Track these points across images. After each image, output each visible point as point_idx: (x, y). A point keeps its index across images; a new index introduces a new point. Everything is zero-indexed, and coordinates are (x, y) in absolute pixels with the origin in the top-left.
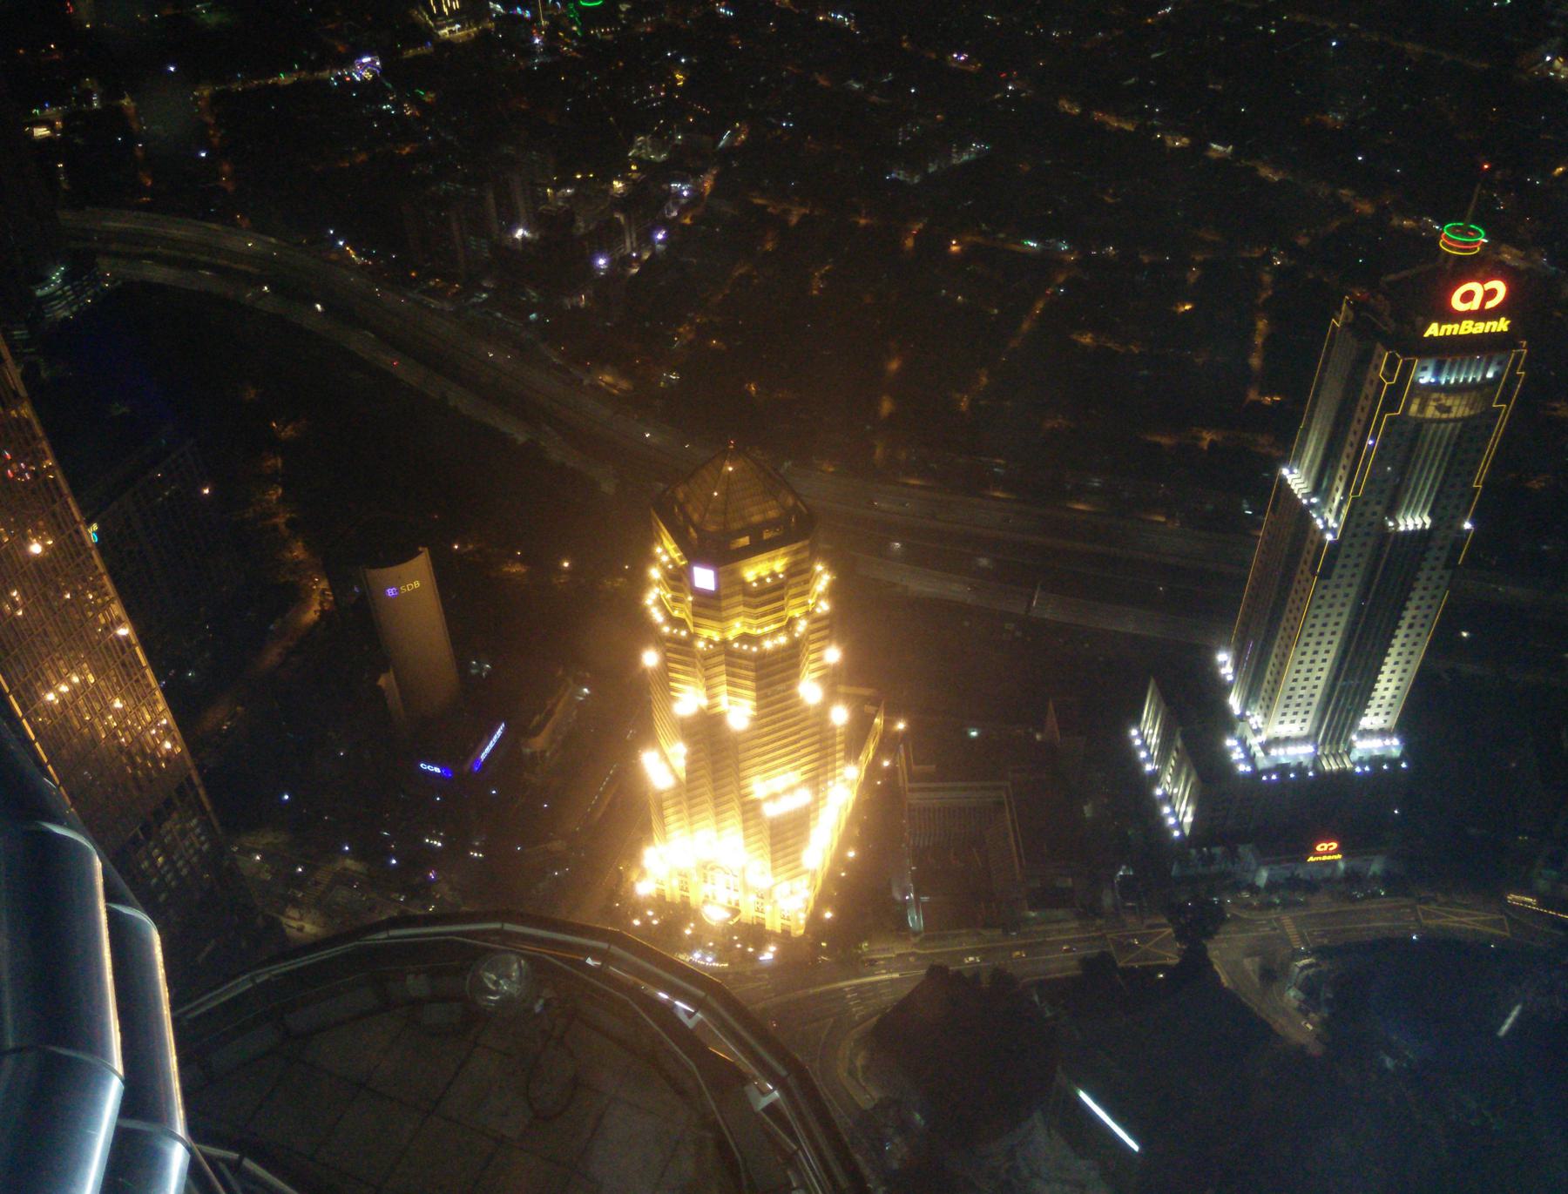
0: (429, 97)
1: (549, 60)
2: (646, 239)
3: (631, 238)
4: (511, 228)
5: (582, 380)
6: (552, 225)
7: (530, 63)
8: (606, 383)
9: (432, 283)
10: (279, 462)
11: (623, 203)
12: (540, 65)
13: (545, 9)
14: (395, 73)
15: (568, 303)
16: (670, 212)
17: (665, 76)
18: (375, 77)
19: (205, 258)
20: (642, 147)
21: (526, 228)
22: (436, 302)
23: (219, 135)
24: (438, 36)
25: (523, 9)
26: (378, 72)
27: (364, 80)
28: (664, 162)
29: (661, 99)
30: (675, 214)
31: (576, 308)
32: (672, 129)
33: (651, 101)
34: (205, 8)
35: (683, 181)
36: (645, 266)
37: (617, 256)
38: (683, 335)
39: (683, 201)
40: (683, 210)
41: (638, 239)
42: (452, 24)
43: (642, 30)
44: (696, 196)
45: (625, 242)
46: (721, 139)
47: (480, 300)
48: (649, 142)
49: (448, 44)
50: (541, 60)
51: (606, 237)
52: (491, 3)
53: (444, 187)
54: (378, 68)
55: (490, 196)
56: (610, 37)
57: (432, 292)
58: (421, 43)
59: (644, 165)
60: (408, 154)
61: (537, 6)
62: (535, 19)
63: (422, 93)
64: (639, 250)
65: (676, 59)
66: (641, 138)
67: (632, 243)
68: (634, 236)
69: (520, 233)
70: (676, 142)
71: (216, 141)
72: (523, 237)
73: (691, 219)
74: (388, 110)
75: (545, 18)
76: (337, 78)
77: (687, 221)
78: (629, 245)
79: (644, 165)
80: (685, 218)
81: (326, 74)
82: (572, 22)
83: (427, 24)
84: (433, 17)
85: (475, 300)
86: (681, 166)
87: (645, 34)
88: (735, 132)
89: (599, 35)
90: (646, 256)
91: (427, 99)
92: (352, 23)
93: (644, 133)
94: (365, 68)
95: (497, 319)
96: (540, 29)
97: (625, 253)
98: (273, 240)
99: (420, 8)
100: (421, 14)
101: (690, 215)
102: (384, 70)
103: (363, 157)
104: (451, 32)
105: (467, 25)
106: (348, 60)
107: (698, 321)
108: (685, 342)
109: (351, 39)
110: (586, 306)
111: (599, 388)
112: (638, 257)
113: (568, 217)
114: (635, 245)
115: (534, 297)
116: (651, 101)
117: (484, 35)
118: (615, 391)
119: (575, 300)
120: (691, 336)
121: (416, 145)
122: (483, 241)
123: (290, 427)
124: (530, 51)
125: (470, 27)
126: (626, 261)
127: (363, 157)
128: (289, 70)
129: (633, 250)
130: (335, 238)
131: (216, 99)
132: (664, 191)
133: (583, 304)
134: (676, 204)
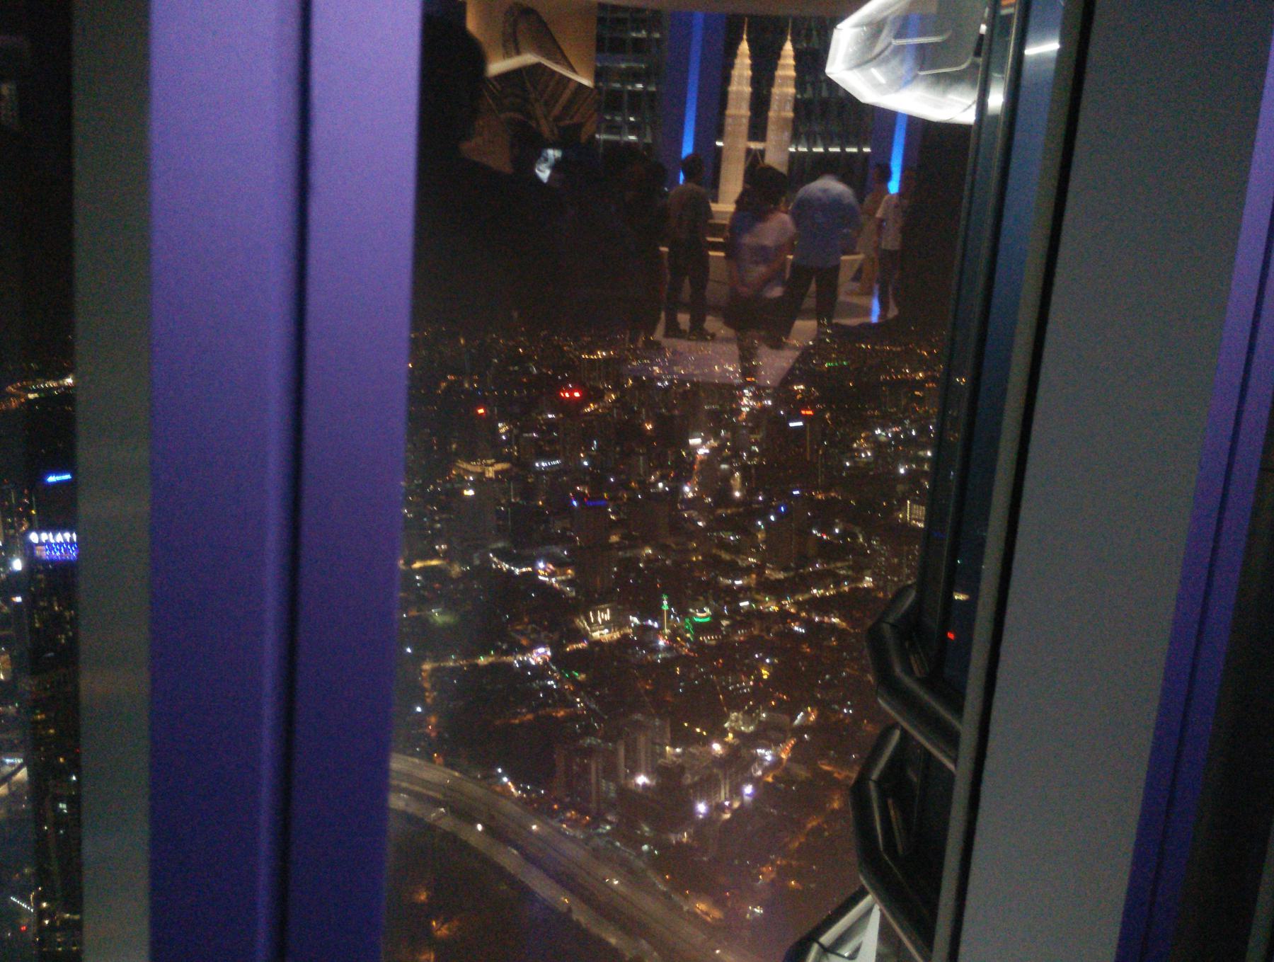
0: (581, 677)
1: (668, 655)
2: (736, 791)
3: (725, 789)
4: (634, 772)
5: (681, 907)
6: (668, 775)
7: (655, 657)
8: (702, 911)
9: (568, 815)
10: (432, 957)
11: (722, 762)
12: (663, 659)
13: (668, 622)
14: (561, 660)
15: (673, 839)
16: (756, 771)
17: (753, 669)
18: (545, 662)
19: (404, 785)
20: (735, 722)
21: (647, 774)
22: (571, 830)
23: (432, 696)
24: (592, 636)
25: (653, 621)
26: (548, 659)
27: (538, 664)
28: (752, 733)
29: (750, 687)
30: (759, 773)
31: (679, 843)
32: (759, 709)
33: (743, 688)
34: (438, 613)
35: (767, 748)
36: (734, 812)
37: (714, 803)
38: (766, 874)
39: (766, 764)
40: (766, 771)
41: (730, 791)
42: (603, 629)
43: (737, 639)
44: (777, 762)
45: (720, 793)
46: (796, 718)
47: (604, 831)
48: (740, 716)
49: (598, 643)
50: (663, 655)
51: (706, 787)
52: (631, 617)
53: (588, 741)
54: (548, 656)
55: (622, 752)
56: (713, 643)
57: (573, 823)
58: (581, 640)
59: (738, 734)
60: (562, 716)
61: (663, 620)
62: (661, 628)
63: (577, 674)
64: (731, 799)
65: (762, 660)
66: (736, 714)
67: (725, 794)
68: (728, 788)
69: (642, 780)
70: (761, 719)
71: (429, 700)
72: (644, 785)
73: (773, 778)
74: (553, 685)
75: (668, 628)
76: (519, 662)
77: (770, 779)
78: (723, 796)
79: (738, 734)
80: (768, 777)
81: (510, 659)
82: (687, 631)
83: (585, 628)
84: (590, 624)
85: (600, 830)
86: (766, 735)
87: (740, 642)
88: (807, 715)
89: (706, 641)
90: (736, 805)
91: (579, 678)
92: (534, 626)
93: (738, 711)
94: (540, 655)
95: (617, 847)
96: (664, 635)
97: (720, 801)
98: (457, 774)
99: (582, 618)
100: (582, 622)
101: (771, 775)
102: (552, 659)
103: (530, 717)
104: (601, 634)
105: (613, 630)
106: (529, 649)
107: (778, 862)
108: (768, 880)
109: (532, 637)
110: (687, 842)
111: (696, 915)
112: (730, 805)
113: (681, 769)
114: (727, 796)
115: (646, 832)
116: (743, 688)
117: (625, 636)
118: (709, 919)
119: (679, 836)
120: (773, 876)
121: (568, 710)
122: (611, 784)
123: (446, 926)
124: (655, 650)
125: (615, 631)
126: (720, 808)
127: (530, 717)
128: (486, 654)
129: (726, 799)
130: (501, 776)
131: (434, 670)
132: (752, 754)
133: (685, 840)
134: (760, 765)
